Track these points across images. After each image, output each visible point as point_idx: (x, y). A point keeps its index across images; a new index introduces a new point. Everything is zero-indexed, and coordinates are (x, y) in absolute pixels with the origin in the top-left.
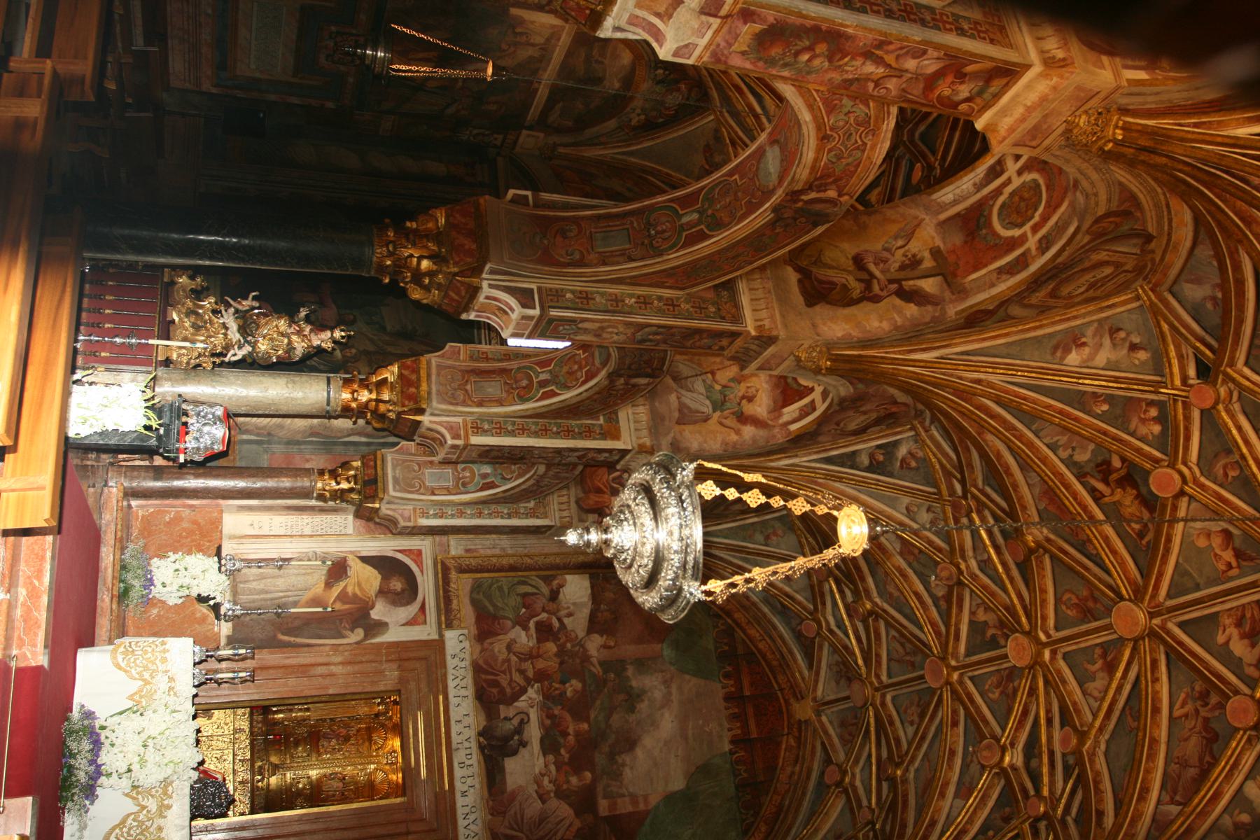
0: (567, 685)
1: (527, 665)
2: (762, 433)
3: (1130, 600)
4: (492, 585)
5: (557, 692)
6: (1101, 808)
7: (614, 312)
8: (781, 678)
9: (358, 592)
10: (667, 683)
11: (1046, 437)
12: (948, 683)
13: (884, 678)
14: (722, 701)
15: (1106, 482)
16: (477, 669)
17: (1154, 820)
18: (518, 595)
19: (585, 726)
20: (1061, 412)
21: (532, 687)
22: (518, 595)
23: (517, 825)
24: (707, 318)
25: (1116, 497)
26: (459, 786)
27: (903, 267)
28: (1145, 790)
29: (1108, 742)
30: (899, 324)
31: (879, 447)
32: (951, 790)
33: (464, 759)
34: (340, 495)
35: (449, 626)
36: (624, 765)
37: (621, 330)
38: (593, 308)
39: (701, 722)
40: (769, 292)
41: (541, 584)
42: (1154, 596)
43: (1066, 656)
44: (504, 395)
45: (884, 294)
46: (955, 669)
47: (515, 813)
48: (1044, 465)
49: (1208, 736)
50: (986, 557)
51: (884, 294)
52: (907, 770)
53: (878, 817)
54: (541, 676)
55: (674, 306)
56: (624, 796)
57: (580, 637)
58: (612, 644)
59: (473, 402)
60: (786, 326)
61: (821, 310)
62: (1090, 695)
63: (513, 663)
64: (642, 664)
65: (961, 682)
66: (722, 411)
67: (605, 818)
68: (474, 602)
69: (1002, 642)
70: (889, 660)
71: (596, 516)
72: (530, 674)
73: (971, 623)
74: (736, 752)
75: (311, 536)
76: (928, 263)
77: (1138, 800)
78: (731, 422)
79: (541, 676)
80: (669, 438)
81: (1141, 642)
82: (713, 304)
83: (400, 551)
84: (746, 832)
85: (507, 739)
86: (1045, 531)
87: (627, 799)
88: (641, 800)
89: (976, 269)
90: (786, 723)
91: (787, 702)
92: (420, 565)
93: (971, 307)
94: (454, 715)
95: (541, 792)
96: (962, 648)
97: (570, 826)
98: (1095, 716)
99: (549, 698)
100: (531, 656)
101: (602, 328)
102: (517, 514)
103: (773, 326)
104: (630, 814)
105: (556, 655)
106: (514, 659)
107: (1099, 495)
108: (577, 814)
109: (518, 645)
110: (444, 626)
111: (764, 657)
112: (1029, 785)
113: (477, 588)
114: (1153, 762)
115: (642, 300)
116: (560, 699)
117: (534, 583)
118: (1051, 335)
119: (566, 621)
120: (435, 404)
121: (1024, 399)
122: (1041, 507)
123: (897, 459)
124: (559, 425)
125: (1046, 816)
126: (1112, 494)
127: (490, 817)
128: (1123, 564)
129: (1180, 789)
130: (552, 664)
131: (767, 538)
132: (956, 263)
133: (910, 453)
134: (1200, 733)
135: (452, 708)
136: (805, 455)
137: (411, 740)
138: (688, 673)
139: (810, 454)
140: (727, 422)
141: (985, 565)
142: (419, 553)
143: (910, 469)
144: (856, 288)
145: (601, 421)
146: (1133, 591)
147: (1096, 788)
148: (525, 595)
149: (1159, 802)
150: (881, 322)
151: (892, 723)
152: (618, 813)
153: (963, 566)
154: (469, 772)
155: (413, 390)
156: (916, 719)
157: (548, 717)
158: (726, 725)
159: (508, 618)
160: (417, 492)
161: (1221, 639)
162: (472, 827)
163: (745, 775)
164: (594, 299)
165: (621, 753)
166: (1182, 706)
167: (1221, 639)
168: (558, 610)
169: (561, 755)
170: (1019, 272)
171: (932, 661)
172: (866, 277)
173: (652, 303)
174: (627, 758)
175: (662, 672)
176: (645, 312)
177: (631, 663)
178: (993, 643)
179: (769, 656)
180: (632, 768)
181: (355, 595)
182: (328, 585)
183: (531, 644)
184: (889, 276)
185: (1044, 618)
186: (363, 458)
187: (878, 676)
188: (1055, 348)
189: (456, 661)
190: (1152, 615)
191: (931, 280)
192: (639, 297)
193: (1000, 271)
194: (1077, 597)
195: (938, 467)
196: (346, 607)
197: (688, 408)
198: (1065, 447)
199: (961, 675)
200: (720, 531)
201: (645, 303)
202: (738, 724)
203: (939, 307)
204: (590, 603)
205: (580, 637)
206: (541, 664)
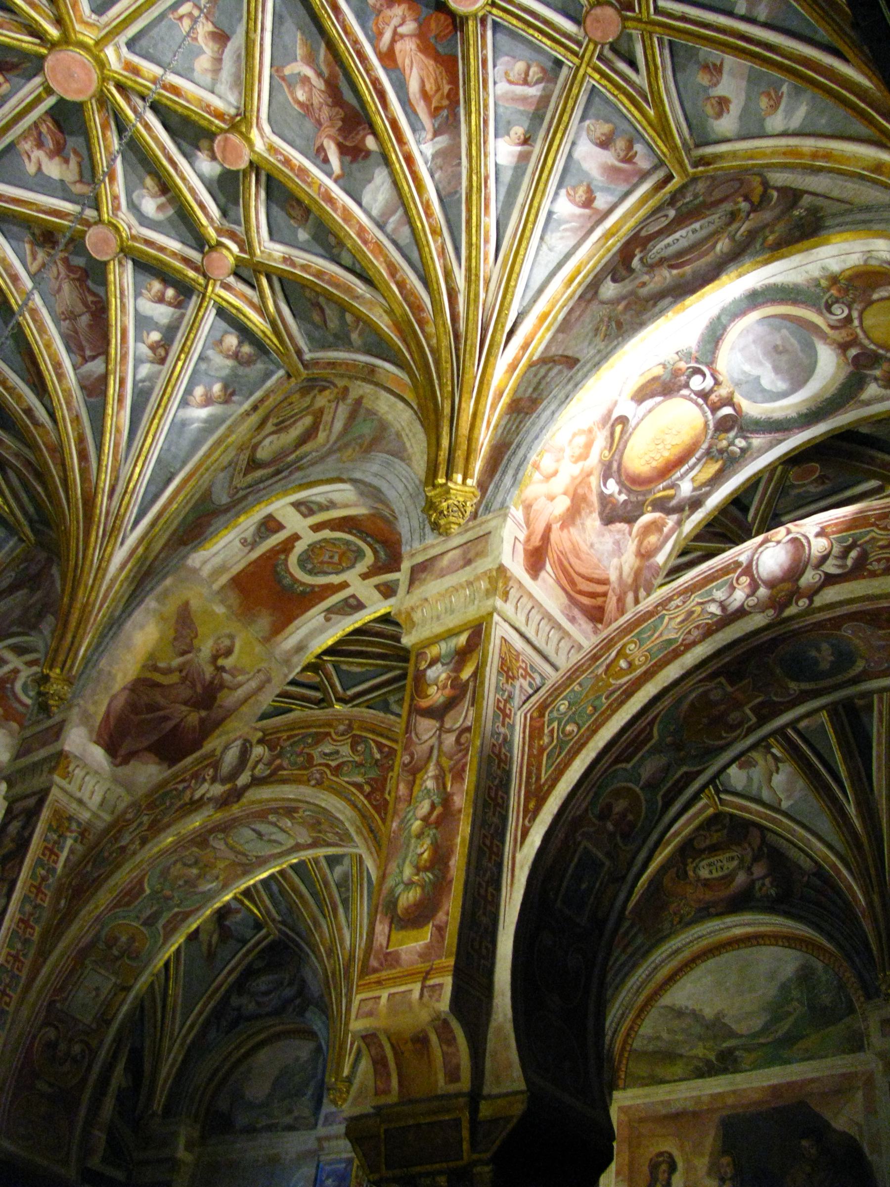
6: (24, 406)
17: (83, 388)
28: (58, 366)
49: (77, 276)
77: (60, 381)
114: (45, 332)
129: (84, 343)
134: (68, 276)
149: (75, 368)
161: (31, 169)
166: (34, 258)
167: (31, 169)
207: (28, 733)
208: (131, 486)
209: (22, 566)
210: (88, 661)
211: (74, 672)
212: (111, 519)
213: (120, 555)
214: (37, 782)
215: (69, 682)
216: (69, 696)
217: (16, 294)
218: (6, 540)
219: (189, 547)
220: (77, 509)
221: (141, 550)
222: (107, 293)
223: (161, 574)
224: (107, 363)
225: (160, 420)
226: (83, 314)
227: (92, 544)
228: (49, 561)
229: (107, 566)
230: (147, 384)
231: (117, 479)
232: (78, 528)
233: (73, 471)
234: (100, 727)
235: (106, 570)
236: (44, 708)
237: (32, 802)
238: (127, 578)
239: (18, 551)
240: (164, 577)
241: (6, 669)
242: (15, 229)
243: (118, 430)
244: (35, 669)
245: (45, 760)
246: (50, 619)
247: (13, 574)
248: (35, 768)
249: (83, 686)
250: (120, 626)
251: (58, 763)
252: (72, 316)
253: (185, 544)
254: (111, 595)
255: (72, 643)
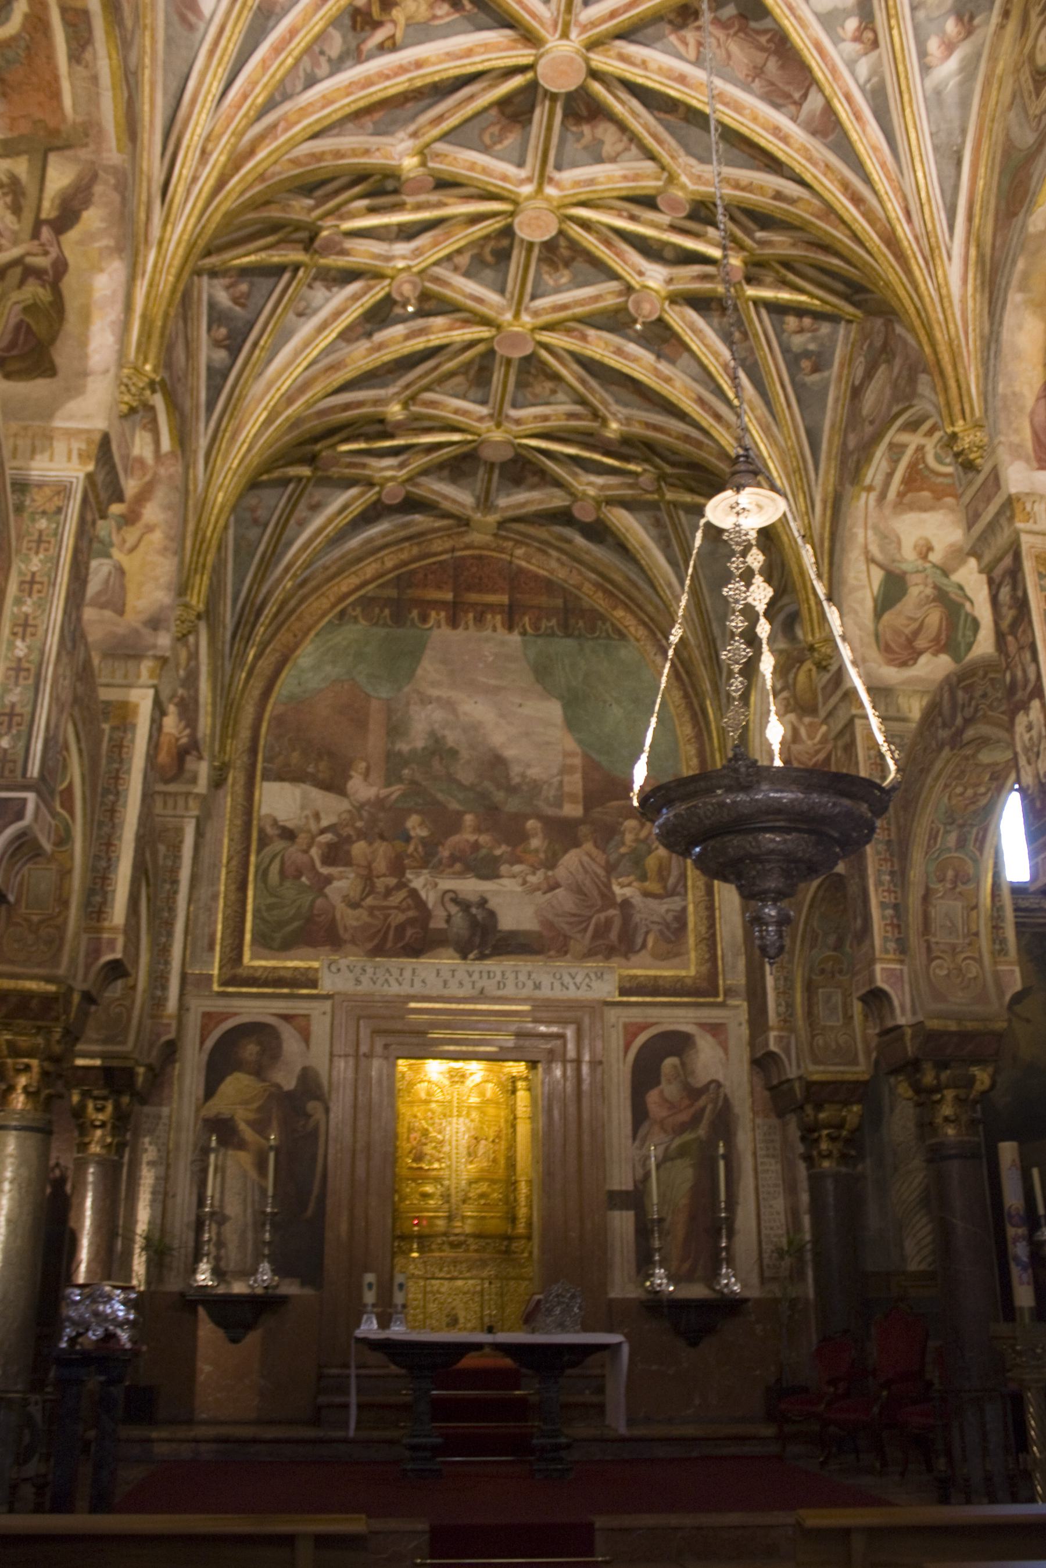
0: (412, 833)
1: (380, 884)
2: (161, 494)
3: (538, 58)
4: (263, 919)
5: (420, 849)
6: (771, 193)
7: (38, 675)
8: (437, 546)
9: (255, 1105)
10: (425, 700)
11: (294, 85)
12: (534, 329)
13: (484, 411)
14: (455, 632)
15: (377, 25)
16: (378, 951)
17: (814, 133)
18: (281, 885)
19: (469, 818)
20: (277, 50)
21: (410, 881)
22: (281, 885)
23: (581, 922)
24: (57, 534)
25: (402, 21)
26: (525, 993)
27: (16, 209)
29: (689, 153)
30: (111, 243)
31: (209, 329)
32: (664, 367)
33: (494, 981)
34: (121, 1122)
35: (314, 984)
36: (523, 775)
37: (61, 671)
38: (29, 709)
39: (481, 665)
40: (26, 428)
41: (268, 850)
42: (542, 23)
43: (559, 168)
44: (54, 866)
45: (54, 252)
46: (517, 315)
47: (570, 924)
48: (333, 102)
49: (736, 28)
50: (395, 229)
51: (54, 252)
52: (614, 414)
53: (656, 467)
54: (398, 867)
55: (32, 582)
56: (561, 782)
57: (350, 807)
58: (363, 765)
59: (60, 913)
60: (88, 417)
61: (62, 355)
62: (618, 154)
63: (376, 903)
64: (396, 729)
65: (536, 314)
66: (112, 545)
67: (587, 809)
68: (286, 946)
69: (505, 242)
70: (464, 397)
71: (189, 758)
72: (392, 881)
73: (467, 274)
74: (524, 626)
75: (168, 1166)
76: (21, 167)
77: (787, 143)
78: (131, 535)
79: (398, 867)
80: (146, 631)
81: (594, 64)
82: (33, 520)
83: (202, 1042)
84: (622, 636)
85: (474, 924)
86: (401, 135)
87: (566, 778)
88: (569, 761)
89: (56, 95)
90: (495, 554)
91: (468, 547)
92: (225, 1016)
93: (117, 124)
94: (437, 990)
95: (545, 886)
96: (493, 297)
97: (589, 855)
98: (652, 157)
99: (428, 860)
100: (368, 879)
101: (58, 699)
102: (175, 870)
103: (84, 437)
104: (585, 777)
105: (370, 844)
106: (369, 901)
107: (388, 44)
108: (576, 844)
109: (352, 894)
110: (314, 992)
111: (405, 564)
112: (697, 269)
113: (264, 941)
114: (744, 108)
115: (19, 630)
116: (430, 846)
117: (267, 860)
118: (168, 23)
119: (325, 823)
120: (61, 971)
121: (245, 97)
122: (370, 126)
123: (230, 309)
124: (106, 791)
125: (746, 263)
126: (394, 22)
127: (568, 956)
128: (487, 47)
129: (787, 88)
130: (382, 853)
131: (256, 522)
132: (35, 123)
133: (227, 288)
134: (728, 35)
135: (427, 992)
136: (197, 441)
137: (464, 1048)
138: (414, 670)
139: (197, 432)
140: (131, 540)
141: (407, 233)
142: (207, 1016)
143: (248, 295)
144: (34, 291)
145: (106, 727)
146: (526, 47)
147: (743, 189)
148: (283, 873)
149: (794, 119)
150: (101, 270)
151: (546, 418)
152: (581, 793)
153: (401, 264)
154: (511, 976)
155: (34, 1003)
156: (549, 385)
157: (451, 866)
158: (488, 632)
159: (313, 902)
160: (130, 1010)
162: (579, 979)
163: (553, 622)
164: (13, 705)
165: (508, 777)
166: (686, 44)
168: (309, 831)
169: (501, 856)
170: (90, 30)
171: (499, 343)
172: (18, 271)
173: (27, 616)
174: (515, 770)
175: (408, 704)
176: (40, 632)
177: (393, 743)
178: (503, 256)
179: (404, 556)
180: (528, 766)
181: (259, 1109)
182: (241, 1145)
183: (352, 876)
184: (26, 234)
185: (505, 178)
186: (69, 1086)
187: (481, 419)
188: (184, 19)
189: (365, 979)
190: (565, 35)
191: (52, 173)
192: (15, 634)
193: (75, 58)
194: (493, 124)
195: (262, 256)
196: (275, 1124)
197: (99, 593)
198: (316, 64)
199: (527, 309)
200: (234, 585)
201: (25, 625)
202: (489, 616)
203: (101, 173)
204: (303, 786)
205: (350, 807)
206: (381, 865)
207: (966, 499)
208: (923, 194)
209: (865, 347)
210: (984, 395)
211: (977, 414)
212: (924, 242)
213: (954, 271)
214: (1002, 539)
215: (978, 426)
216: (986, 440)
217: (693, 93)
218: (835, 332)
219: (1021, 215)
220: (884, 255)
221: (973, 252)
222: (775, 20)
223: (1009, 261)
224: (821, 90)
225: (911, 106)
226: (767, 59)
227: (920, 279)
228: (888, 323)
229: (948, 290)
230: (875, 79)
231: (905, 198)
232: (896, 273)
233: (856, 220)
234: (1035, 451)
235: (949, 296)
236: (969, 466)
237: (1008, 561)
238: (975, 289)
239: (852, 335)
240: (1014, 262)
241: (910, 452)
242: (650, 31)
243: (875, 149)
244: (938, 435)
245: (998, 514)
246: (923, 378)
247: (862, 359)
248: (992, 526)
249: (995, 422)
250: (997, 341)
251: (1013, 510)
252: (758, 72)
253: (1015, 214)
254: (970, 316)
255: (959, 387)
